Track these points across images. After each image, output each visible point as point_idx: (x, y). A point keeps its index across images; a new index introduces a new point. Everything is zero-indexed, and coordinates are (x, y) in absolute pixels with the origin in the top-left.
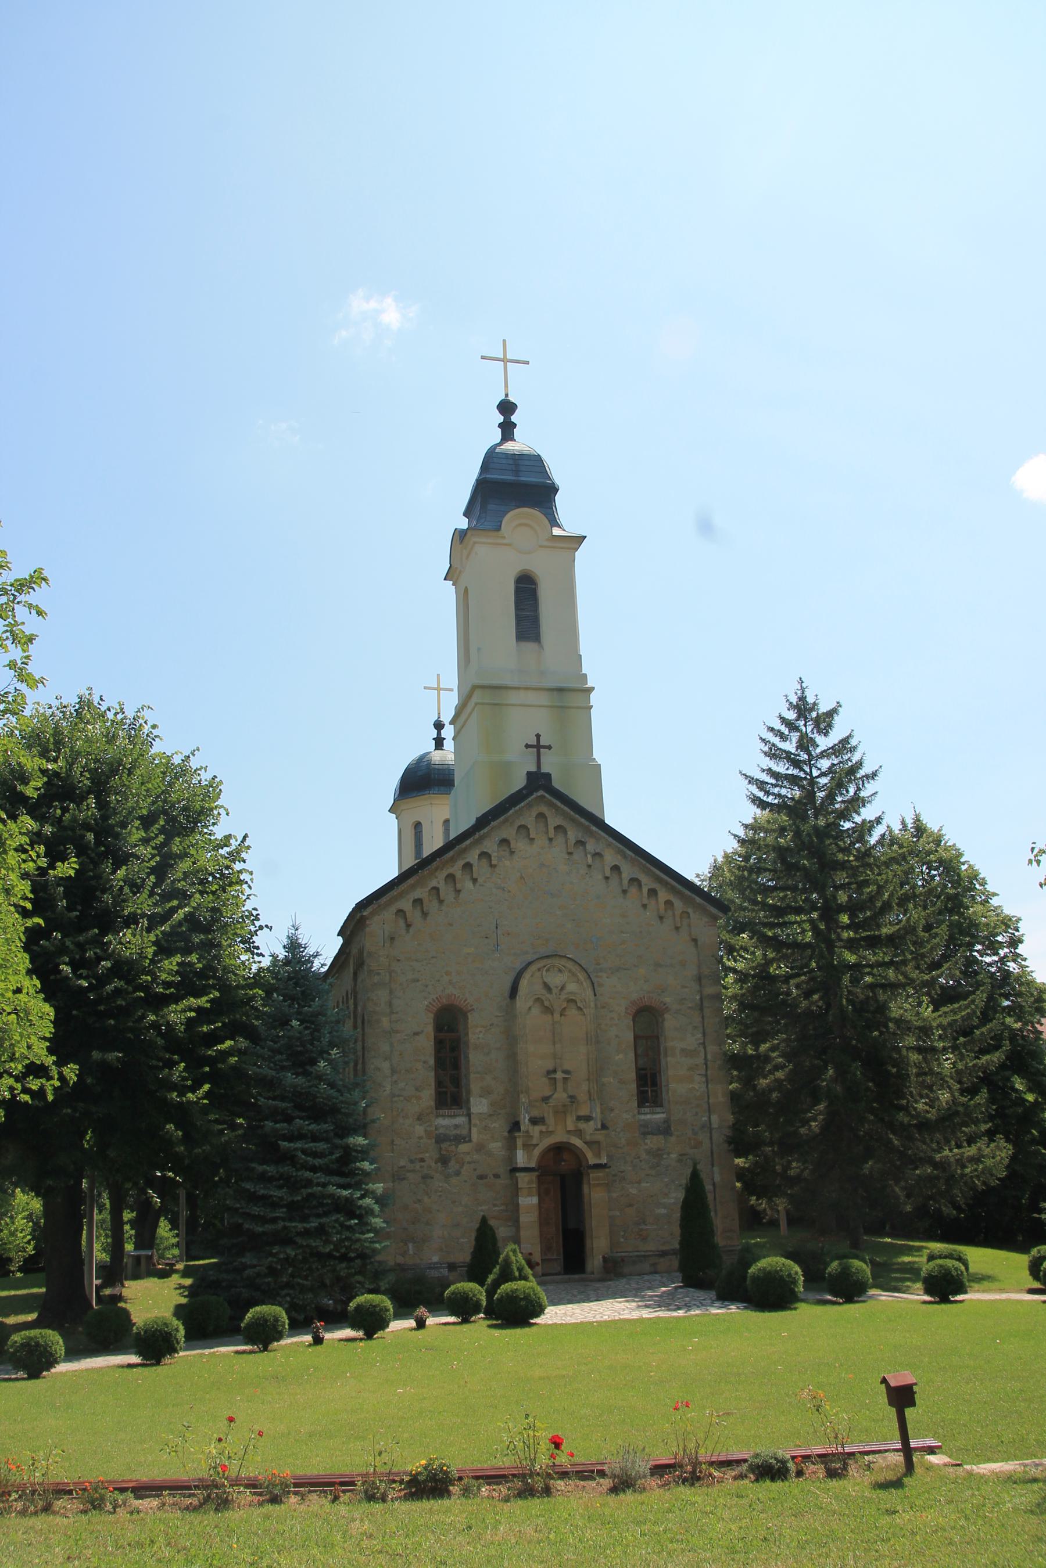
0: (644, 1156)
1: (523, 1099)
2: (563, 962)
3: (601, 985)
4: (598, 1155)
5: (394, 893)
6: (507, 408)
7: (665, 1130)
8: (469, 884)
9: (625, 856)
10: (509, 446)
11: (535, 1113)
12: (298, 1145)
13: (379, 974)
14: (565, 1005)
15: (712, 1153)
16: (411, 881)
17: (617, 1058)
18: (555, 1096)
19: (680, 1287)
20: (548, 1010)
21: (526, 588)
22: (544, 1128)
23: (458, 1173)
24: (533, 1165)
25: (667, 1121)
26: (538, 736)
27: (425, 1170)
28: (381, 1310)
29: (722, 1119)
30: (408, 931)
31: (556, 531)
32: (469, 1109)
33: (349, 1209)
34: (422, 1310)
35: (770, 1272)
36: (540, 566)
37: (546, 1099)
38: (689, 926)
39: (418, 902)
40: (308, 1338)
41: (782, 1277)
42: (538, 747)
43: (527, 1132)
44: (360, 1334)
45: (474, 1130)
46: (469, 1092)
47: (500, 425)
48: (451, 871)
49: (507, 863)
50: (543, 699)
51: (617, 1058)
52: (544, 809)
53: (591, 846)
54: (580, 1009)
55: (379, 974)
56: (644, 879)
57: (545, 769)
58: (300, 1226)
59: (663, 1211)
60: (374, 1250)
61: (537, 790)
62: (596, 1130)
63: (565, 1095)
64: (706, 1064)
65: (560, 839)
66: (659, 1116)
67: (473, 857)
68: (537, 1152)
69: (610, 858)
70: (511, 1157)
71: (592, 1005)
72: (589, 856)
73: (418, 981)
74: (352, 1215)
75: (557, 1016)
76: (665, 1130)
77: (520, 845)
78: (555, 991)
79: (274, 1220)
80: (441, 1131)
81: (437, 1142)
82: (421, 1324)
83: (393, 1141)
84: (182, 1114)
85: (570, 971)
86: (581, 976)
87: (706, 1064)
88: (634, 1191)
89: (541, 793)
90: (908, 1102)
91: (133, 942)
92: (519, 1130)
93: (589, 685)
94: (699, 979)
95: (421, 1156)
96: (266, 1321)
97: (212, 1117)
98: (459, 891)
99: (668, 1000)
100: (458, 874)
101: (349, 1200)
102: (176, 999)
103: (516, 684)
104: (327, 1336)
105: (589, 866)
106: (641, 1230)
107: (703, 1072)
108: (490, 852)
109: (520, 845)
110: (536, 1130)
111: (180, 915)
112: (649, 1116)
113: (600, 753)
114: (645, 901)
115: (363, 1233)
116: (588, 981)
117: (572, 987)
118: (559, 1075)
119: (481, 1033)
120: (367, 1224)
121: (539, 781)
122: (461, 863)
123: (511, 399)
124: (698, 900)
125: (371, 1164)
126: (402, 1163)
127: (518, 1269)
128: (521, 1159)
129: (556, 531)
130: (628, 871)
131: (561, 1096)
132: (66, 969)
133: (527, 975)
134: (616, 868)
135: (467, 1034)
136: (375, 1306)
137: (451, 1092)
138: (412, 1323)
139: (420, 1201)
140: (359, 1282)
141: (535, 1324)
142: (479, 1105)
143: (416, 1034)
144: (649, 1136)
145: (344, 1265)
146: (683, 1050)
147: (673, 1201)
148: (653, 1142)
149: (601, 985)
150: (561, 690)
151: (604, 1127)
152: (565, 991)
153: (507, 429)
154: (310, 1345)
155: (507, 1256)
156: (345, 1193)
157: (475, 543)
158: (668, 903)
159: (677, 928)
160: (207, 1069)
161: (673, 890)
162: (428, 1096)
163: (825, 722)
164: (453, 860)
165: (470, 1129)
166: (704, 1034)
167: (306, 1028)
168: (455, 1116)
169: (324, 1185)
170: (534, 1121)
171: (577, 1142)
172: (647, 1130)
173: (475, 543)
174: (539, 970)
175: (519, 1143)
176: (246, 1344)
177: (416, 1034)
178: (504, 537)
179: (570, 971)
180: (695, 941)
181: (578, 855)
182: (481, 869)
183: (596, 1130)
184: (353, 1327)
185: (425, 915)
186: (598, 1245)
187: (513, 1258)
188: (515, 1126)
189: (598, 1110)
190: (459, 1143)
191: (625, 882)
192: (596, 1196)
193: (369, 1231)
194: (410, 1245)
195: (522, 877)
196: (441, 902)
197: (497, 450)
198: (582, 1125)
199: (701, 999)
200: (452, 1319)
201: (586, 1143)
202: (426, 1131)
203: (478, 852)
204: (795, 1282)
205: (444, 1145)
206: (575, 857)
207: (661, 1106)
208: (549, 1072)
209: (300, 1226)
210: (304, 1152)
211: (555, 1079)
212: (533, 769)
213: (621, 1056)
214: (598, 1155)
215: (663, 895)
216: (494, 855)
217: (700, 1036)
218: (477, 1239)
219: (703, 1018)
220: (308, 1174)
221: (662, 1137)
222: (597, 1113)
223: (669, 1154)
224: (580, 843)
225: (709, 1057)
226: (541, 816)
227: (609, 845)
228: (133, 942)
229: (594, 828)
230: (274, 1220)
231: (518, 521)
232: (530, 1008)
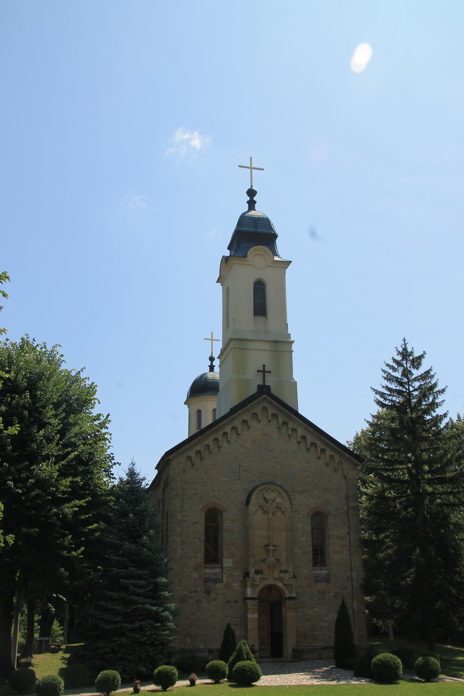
1: (251, 560)
2: (274, 486)
4: (291, 592)
5: (186, 447)
6: (251, 193)
7: (327, 579)
8: (225, 444)
9: (308, 431)
10: (252, 213)
11: (258, 568)
12: (130, 581)
13: (176, 490)
14: (275, 510)
15: (353, 593)
16: (195, 441)
17: (302, 539)
18: (269, 559)
19: (334, 668)
20: (266, 512)
21: (260, 288)
22: (262, 576)
23: (215, 599)
24: (256, 596)
25: (328, 575)
26: (264, 366)
27: (197, 598)
28: (171, 674)
29: (359, 575)
30: (192, 467)
31: (276, 258)
32: (222, 564)
33: (156, 617)
34: (193, 675)
35: (384, 662)
36: (268, 276)
37: (263, 560)
39: (198, 452)
40: (131, 689)
41: (390, 665)
42: (264, 372)
43: (253, 578)
44: (160, 688)
45: (225, 576)
46: (222, 556)
47: (248, 202)
48: (216, 436)
49: (246, 433)
50: (267, 346)
51: (302, 539)
52: (266, 405)
53: (290, 425)
54: (283, 512)
55: (176, 490)
56: (318, 443)
57: (267, 384)
58: (129, 626)
59: (326, 624)
60: (169, 641)
61: (263, 394)
63: (273, 559)
64: (350, 544)
65: (275, 421)
66: (324, 572)
67: (228, 429)
68: (258, 589)
69: (301, 431)
70: (244, 592)
71: (290, 510)
72: (290, 430)
73: (197, 494)
74: (157, 621)
75: (270, 516)
76: (327, 579)
77: (253, 423)
78: (269, 502)
79: (116, 623)
80: (207, 576)
81: (204, 582)
82: (193, 683)
83: (181, 581)
84: (69, 563)
85: (278, 491)
86: (284, 494)
87: (350, 544)
88: (310, 613)
89: (265, 396)
90: (460, 569)
91: (46, 469)
92: (249, 577)
93: (292, 339)
94: (347, 498)
96: (109, 679)
97: (85, 565)
98: (220, 447)
99: (330, 508)
100: (220, 438)
101: (156, 612)
102: (68, 500)
103: (253, 338)
104: (142, 688)
105: (290, 436)
107: (349, 549)
108: (237, 426)
109: (253, 423)
110: (258, 577)
111: (72, 455)
112: (318, 572)
113: (296, 376)
114: (319, 455)
115: (163, 631)
117: (279, 500)
118: (271, 548)
119: (230, 524)
120: (166, 626)
121: (263, 390)
122: (221, 432)
123: (254, 188)
124: (347, 455)
125: (169, 593)
126: (185, 593)
127: (246, 654)
128: (249, 592)
129: (276, 258)
130: (310, 439)
131: (272, 559)
132: (11, 483)
133: (255, 493)
134: (304, 437)
135: (222, 524)
136: (168, 672)
137: (213, 555)
138: (188, 682)
139: (194, 614)
140: (160, 659)
141: (255, 685)
142: (228, 563)
145: (152, 648)
147: (331, 619)
148: (321, 586)
150: (277, 342)
151: (294, 577)
152: (275, 503)
153: (252, 204)
154: (132, 693)
155: (241, 646)
156: (155, 608)
157: (233, 263)
158: (331, 456)
159: (336, 470)
160: (84, 539)
161: (334, 450)
162: (200, 557)
163: (417, 362)
164: (217, 430)
165: (222, 575)
166: (349, 528)
167: (137, 518)
168: (215, 568)
169: (143, 604)
170: (257, 572)
171: (280, 584)
172: (317, 579)
173: (233, 263)
174: (262, 490)
175: (249, 584)
176: (97, 692)
177: (195, 523)
178: (248, 261)
179: (278, 491)
180: (345, 477)
181: (284, 430)
182: (232, 436)
183: (290, 578)
184: (156, 684)
185: (202, 459)
186: (290, 642)
187: (244, 647)
188: (247, 575)
189: (292, 567)
191: (309, 445)
192: (289, 615)
193: (166, 630)
194: (188, 638)
195: (254, 441)
196: (210, 453)
197: (246, 215)
198: (282, 575)
199: (348, 509)
200: (209, 681)
202: (198, 576)
203: (231, 426)
204: (398, 668)
205: (208, 584)
206: (282, 430)
207: (325, 566)
208: (265, 546)
209: (129, 626)
210: (133, 585)
211: (269, 549)
212: (261, 383)
213: (304, 538)
214: (291, 592)
215: (329, 452)
216: (240, 428)
217: (347, 529)
218: (225, 636)
219: (349, 519)
220: (135, 597)
222: (291, 569)
224: (285, 423)
225: (352, 540)
226: (265, 408)
227: (300, 425)
228: (46, 469)
229: (293, 416)
230: (116, 623)
231: (256, 253)
232: (256, 511)
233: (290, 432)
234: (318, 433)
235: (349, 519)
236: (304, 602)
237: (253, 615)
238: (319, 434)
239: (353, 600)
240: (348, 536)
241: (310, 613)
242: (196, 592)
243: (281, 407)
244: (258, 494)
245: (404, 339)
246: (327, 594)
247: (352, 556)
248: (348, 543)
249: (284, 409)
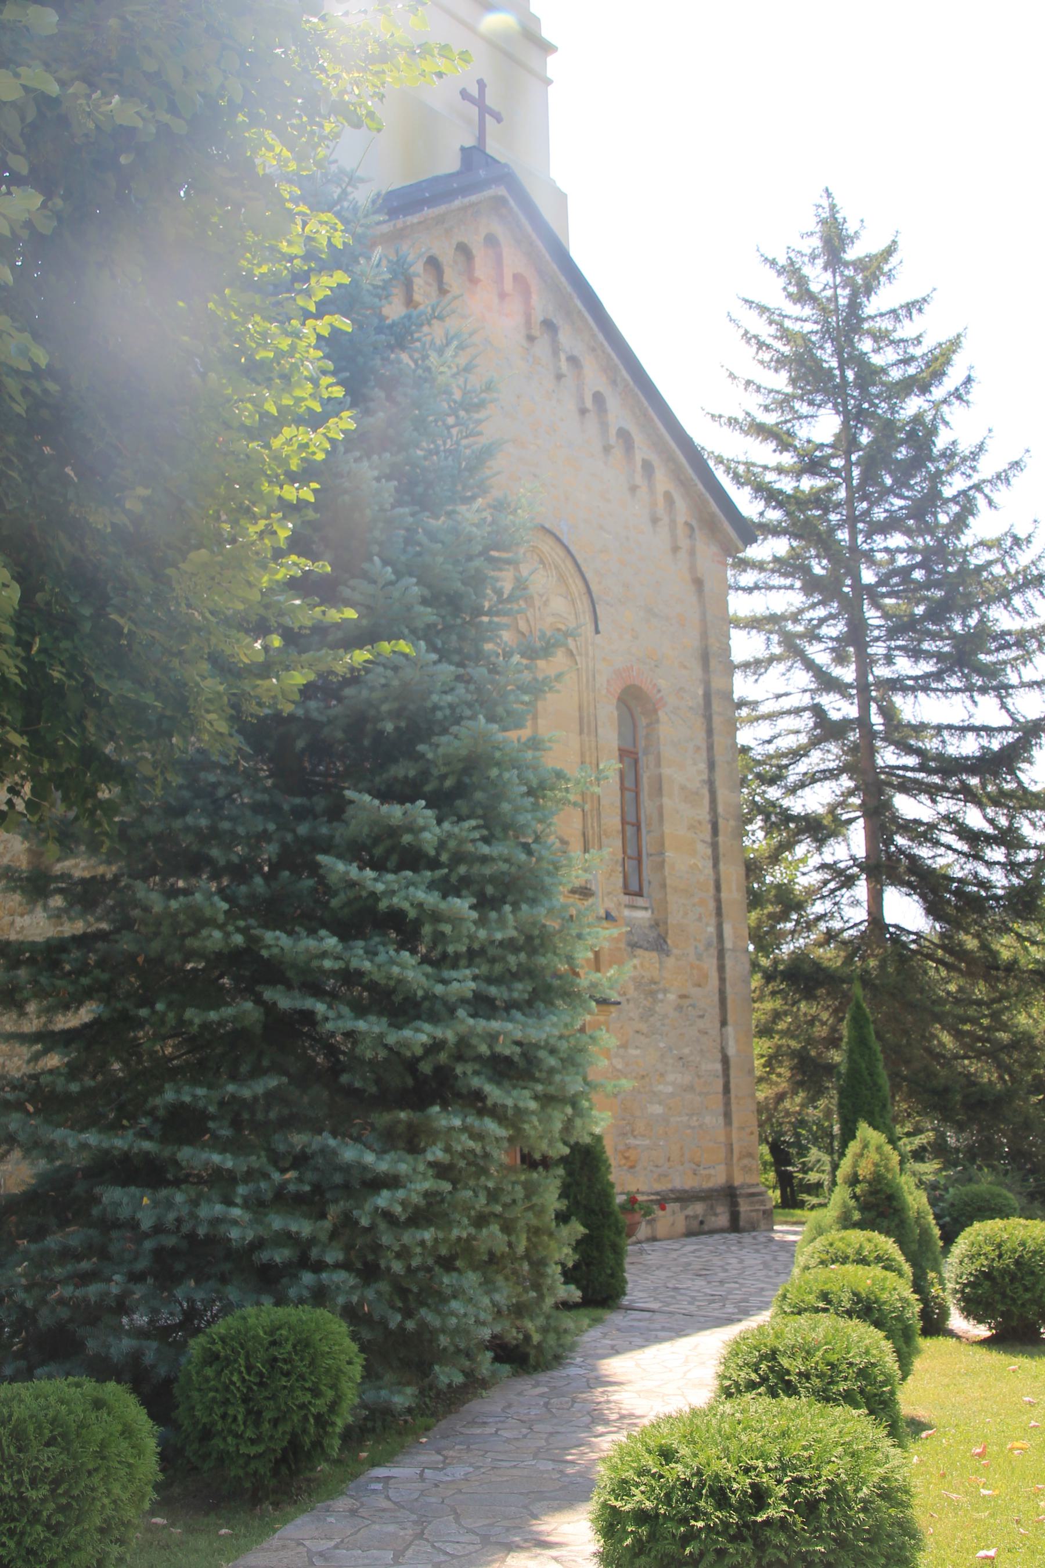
9: (614, 382)
38: (692, 553)
53: (565, 337)
59: (657, 1109)
86: (576, 586)
99: (662, 683)
106: (628, 1147)
107: (708, 839)
116: (585, 599)
144: (639, 952)
146: (683, 788)
163: (873, 271)
166: (711, 766)
180: (698, 583)
191: (613, 431)
217: (703, 766)
219: (710, 732)
221: (655, 954)
223: (665, 991)
224: (549, 325)
225: (720, 809)
229: (579, 304)
233: (564, 365)
234: (643, 399)
235: (710, 732)
238: (646, 404)
239: (724, 1023)
240: (705, 791)
245: (827, 190)
246: (660, 996)
247: (722, 867)
248: (708, 817)
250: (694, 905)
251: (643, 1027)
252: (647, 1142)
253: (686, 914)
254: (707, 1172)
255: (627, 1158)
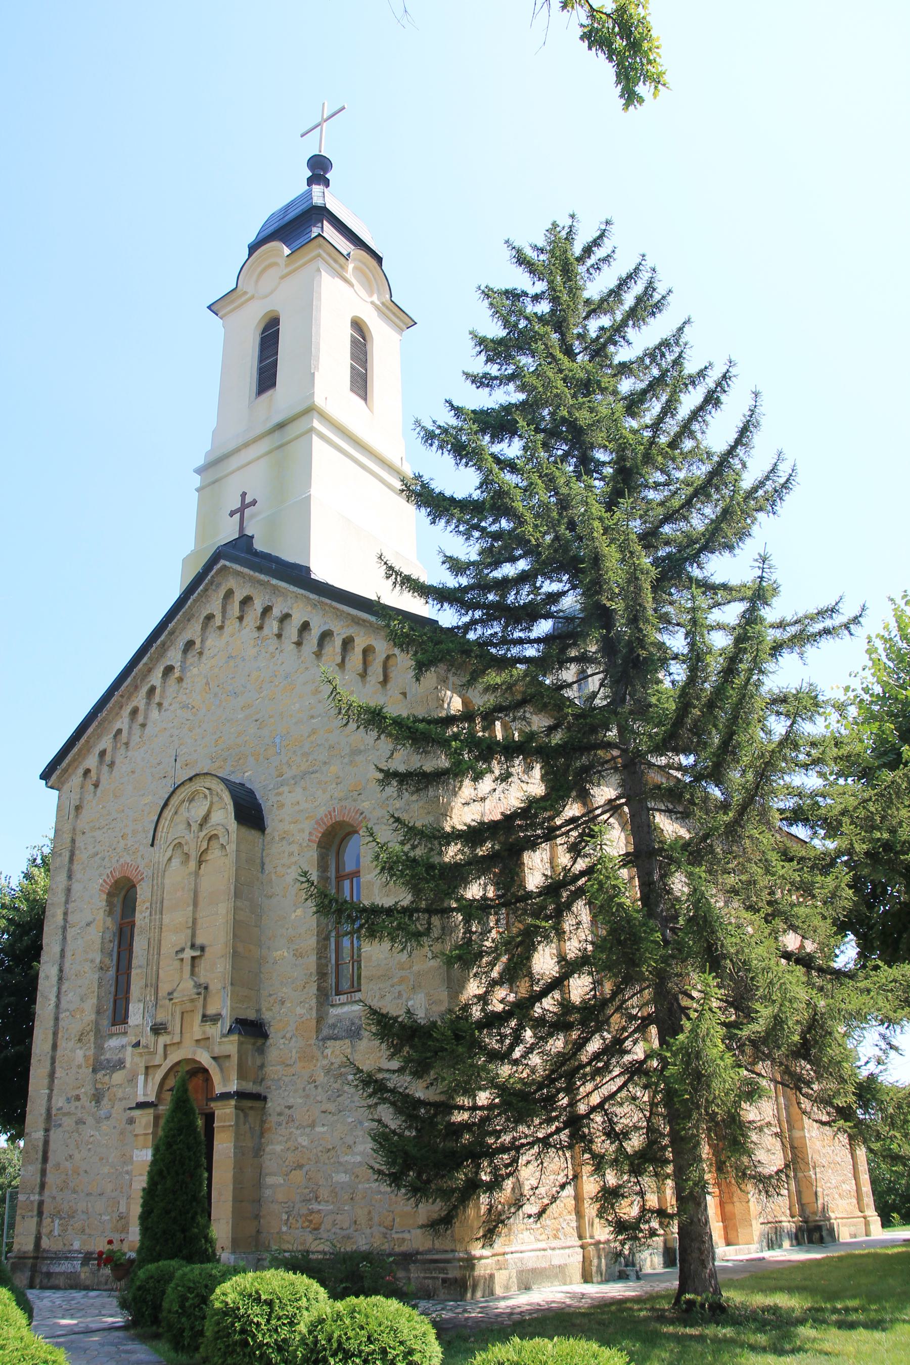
0: (321, 1078)
3: (281, 806)
59: (343, 1178)
62: (223, 1036)
88: (304, 1141)
89: (222, 562)
95: (77, 1092)
99: (365, 805)
106: (312, 1212)
112: (346, 1009)
143: (88, 925)
149: (281, 806)
150: (281, 426)
178: (245, 293)
190: (113, 1072)
201: (214, 1058)
203: (162, 669)
221: (347, 1041)
232: (170, 859)
236: (290, 1107)
237: (144, 1152)
238: (328, 601)
241: (305, 1143)
242: (78, 1098)
243: (252, 573)
244: (176, 813)
249: (257, 574)
250: (392, 986)
251: (331, 1107)
252: (331, 1207)
253: (383, 997)
254: (400, 1236)
255: (311, 1221)
